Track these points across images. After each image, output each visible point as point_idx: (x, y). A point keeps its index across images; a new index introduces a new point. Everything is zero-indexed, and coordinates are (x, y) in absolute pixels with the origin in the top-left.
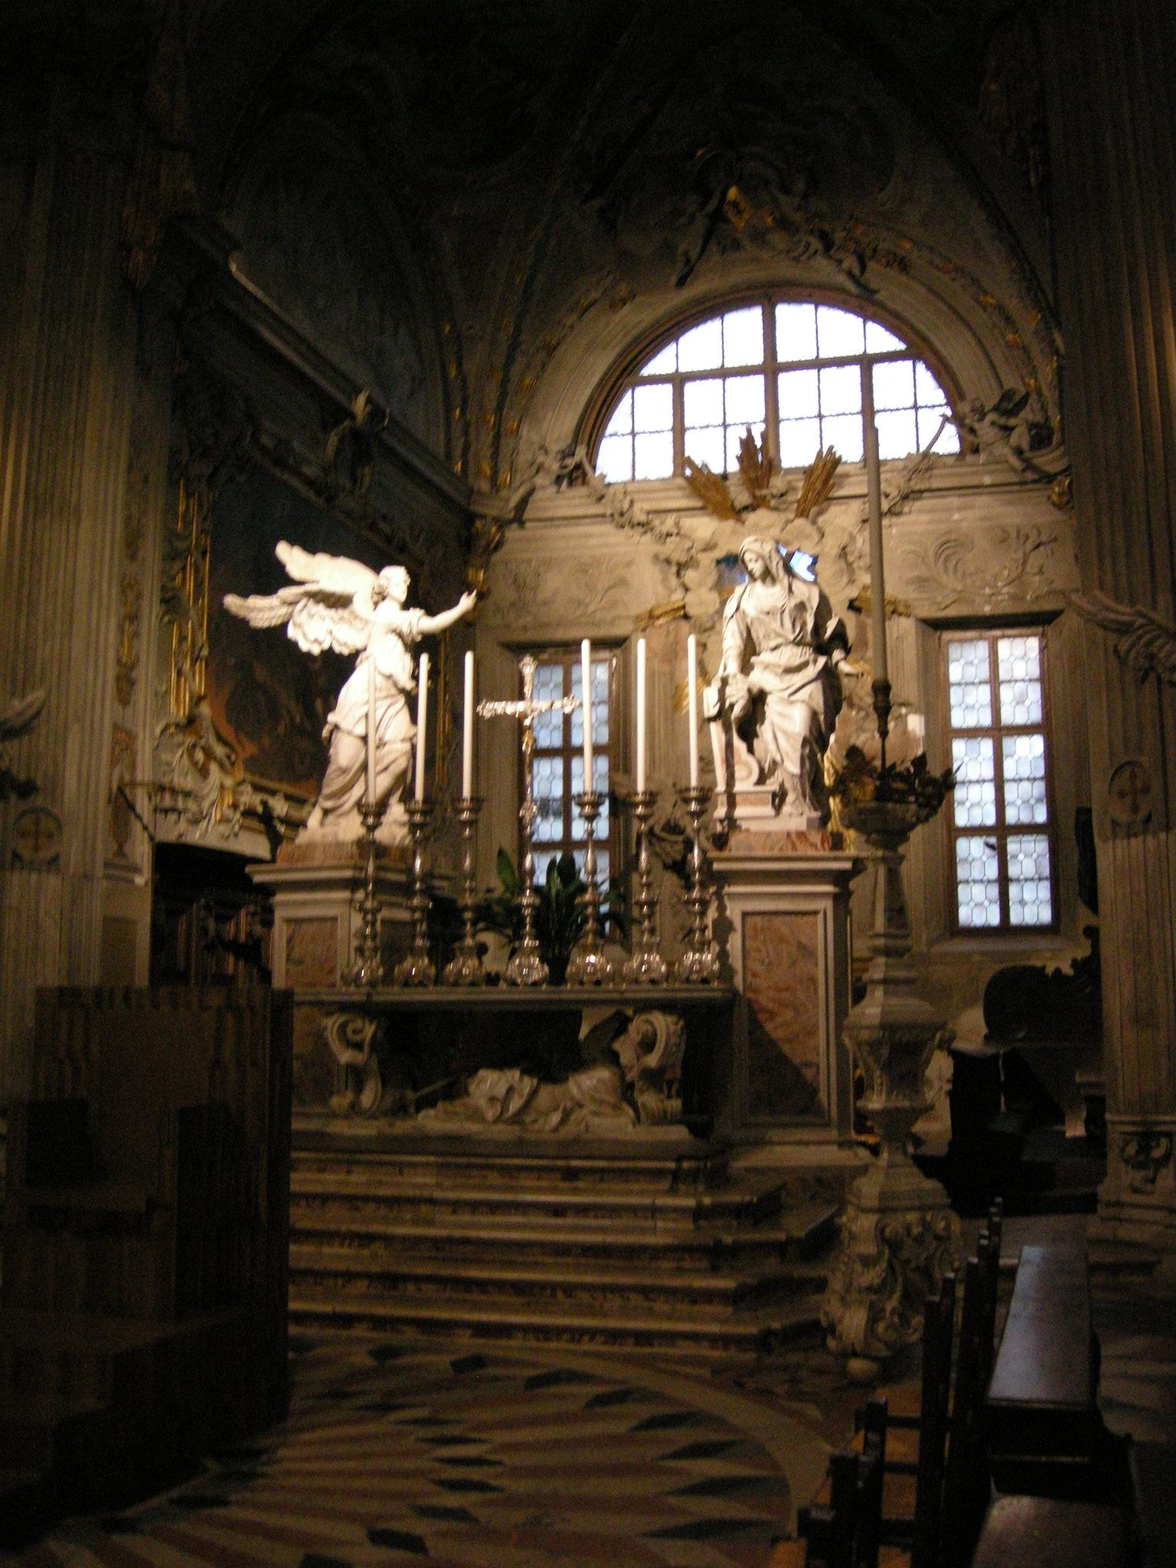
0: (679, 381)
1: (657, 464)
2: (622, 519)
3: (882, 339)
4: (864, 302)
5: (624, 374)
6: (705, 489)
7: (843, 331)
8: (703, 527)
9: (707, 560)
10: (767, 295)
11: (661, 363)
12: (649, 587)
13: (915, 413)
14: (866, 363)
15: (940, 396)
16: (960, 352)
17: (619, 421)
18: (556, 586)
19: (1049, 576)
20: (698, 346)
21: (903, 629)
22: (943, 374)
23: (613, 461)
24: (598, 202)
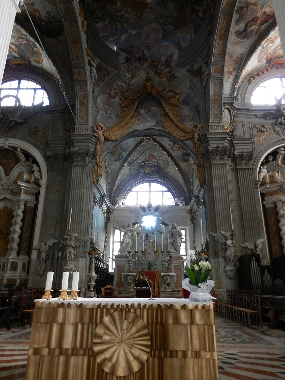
0: (137, 192)
10: (150, 181)
14: (163, 192)
15: (172, 197)
24: (129, 167)
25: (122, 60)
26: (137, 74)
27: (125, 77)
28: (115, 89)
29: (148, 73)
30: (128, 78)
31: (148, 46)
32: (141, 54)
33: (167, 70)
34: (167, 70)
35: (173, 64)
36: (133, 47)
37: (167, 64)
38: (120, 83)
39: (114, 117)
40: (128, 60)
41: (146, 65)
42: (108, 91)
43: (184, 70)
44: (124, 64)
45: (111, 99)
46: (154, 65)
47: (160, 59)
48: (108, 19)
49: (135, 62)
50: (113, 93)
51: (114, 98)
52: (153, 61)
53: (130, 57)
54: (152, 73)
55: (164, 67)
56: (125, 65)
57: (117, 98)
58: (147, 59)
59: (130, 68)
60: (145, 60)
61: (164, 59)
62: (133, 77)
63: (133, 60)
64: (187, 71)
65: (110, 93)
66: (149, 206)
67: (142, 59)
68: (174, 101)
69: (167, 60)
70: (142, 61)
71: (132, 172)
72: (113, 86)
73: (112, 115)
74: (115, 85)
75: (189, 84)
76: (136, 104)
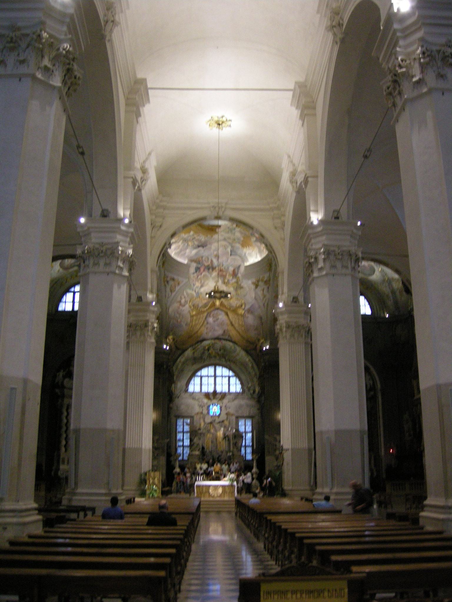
1: (197, 389)
2: (194, 399)
3: (231, 373)
4: (230, 369)
5: (194, 375)
6: (207, 395)
7: (226, 372)
8: (205, 401)
9: (206, 406)
10: (215, 365)
11: (199, 374)
12: (197, 409)
13: (236, 387)
16: (243, 377)
17: (192, 382)
18: (183, 408)
19: (254, 411)
20: (204, 372)
21: (234, 418)
22: (240, 380)
23: (191, 389)
25: (192, 270)
26: (206, 283)
27: (194, 285)
28: (185, 297)
29: (217, 282)
30: (197, 287)
31: (217, 257)
32: (209, 262)
33: (234, 280)
34: (234, 280)
35: (239, 275)
36: (202, 257)
37: (235, 274)
38: (189, 291)
39: (184, 325)
40: (197, 269)
41: (215, 274)
42: (179, 299)
43: (250, 282)
44: (194, 273)
45: (181, 307)
46: (222, 274)
47: (228, 268)
48: (181, 241)
49: (204, 270)
50: (183, 301)
51: (184, 306)
52: (221, 270)
53: (199, 266)
54: (220, 283)
55: (231, 278)
56: (195, 274)
57: (187, 306)
58: (215, 268)
59: (199, 277)
60: (213, 269)
61: (231, 269)
62: (202, 286)
63: (202, 270)
64: (253, 283)
65: (180, 302)
66: (215, 393)
67: (210, 268)
68: (241, 311)
69: (234, 271)
70: (211, 270)
71: (196, 355)
72: (183, 294)
73: (182, 323)
74: (185, 294)
75: (253, 295)
76: (205, 314)
